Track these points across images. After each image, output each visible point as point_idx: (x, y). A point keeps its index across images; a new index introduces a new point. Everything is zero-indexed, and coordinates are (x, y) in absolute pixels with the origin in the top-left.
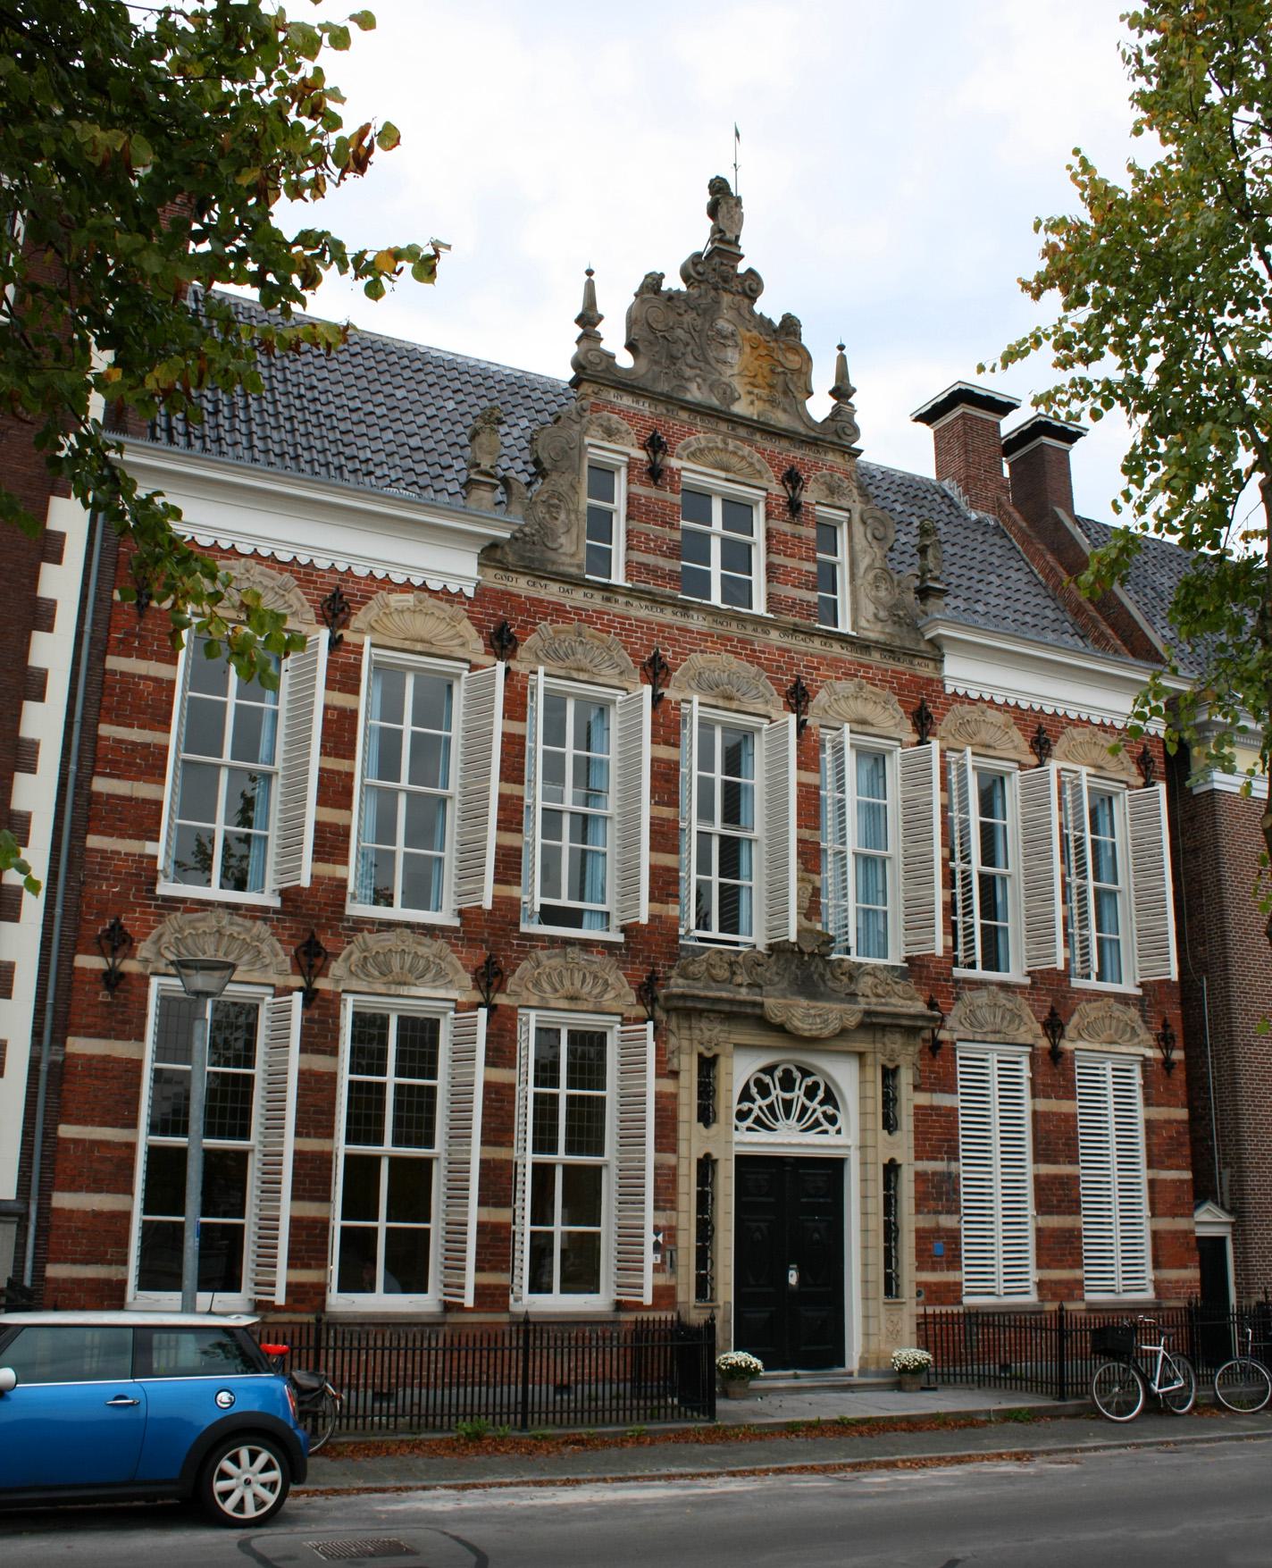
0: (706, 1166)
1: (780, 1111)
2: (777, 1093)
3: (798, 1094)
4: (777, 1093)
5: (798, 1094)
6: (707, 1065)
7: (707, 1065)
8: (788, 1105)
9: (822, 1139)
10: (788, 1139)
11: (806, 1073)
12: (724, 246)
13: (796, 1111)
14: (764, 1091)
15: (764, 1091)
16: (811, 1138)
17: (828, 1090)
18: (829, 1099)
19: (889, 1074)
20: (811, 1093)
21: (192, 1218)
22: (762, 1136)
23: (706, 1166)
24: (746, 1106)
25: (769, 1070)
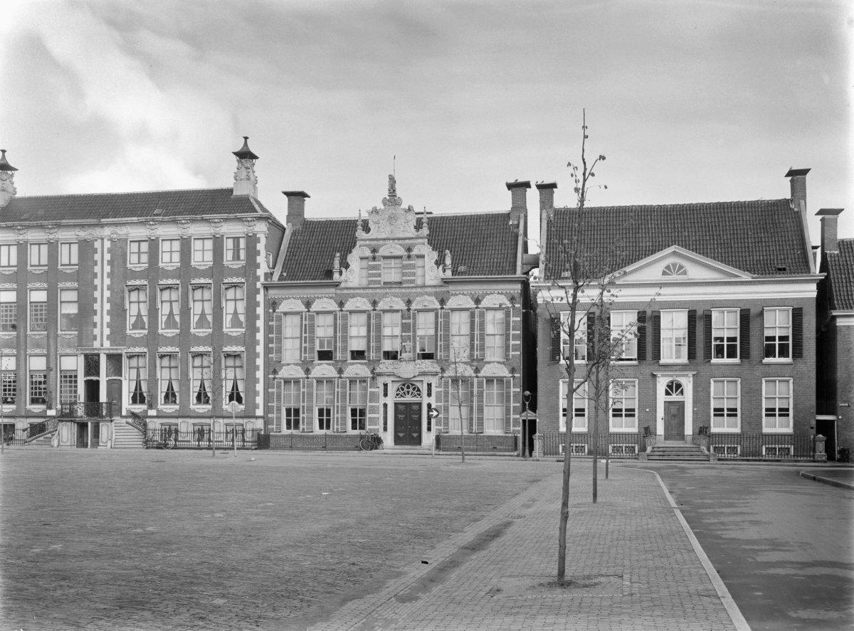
0: (385, 405)
1: (406, 393)
2: (406, 390)
3: (411, 390)
4: (406, 390)
5: (411, 390)
6: (386, 385)
7: (386, 385)
8: (408, 392)
9: (417, 399)
10: (408, 399)
11: (413, 385)
12: (392, 191)
13: (410, 393)
14: (403, 389)
15: (403, 389)
16: (414, 399)
17: (418, 388)
18: (419, 390)
19: (429, 385)
20: (414, 389)
21: (325, 418)
22: (402, 399)
23: (385, 405)
24: (398, 392)
25: (404, 385)
